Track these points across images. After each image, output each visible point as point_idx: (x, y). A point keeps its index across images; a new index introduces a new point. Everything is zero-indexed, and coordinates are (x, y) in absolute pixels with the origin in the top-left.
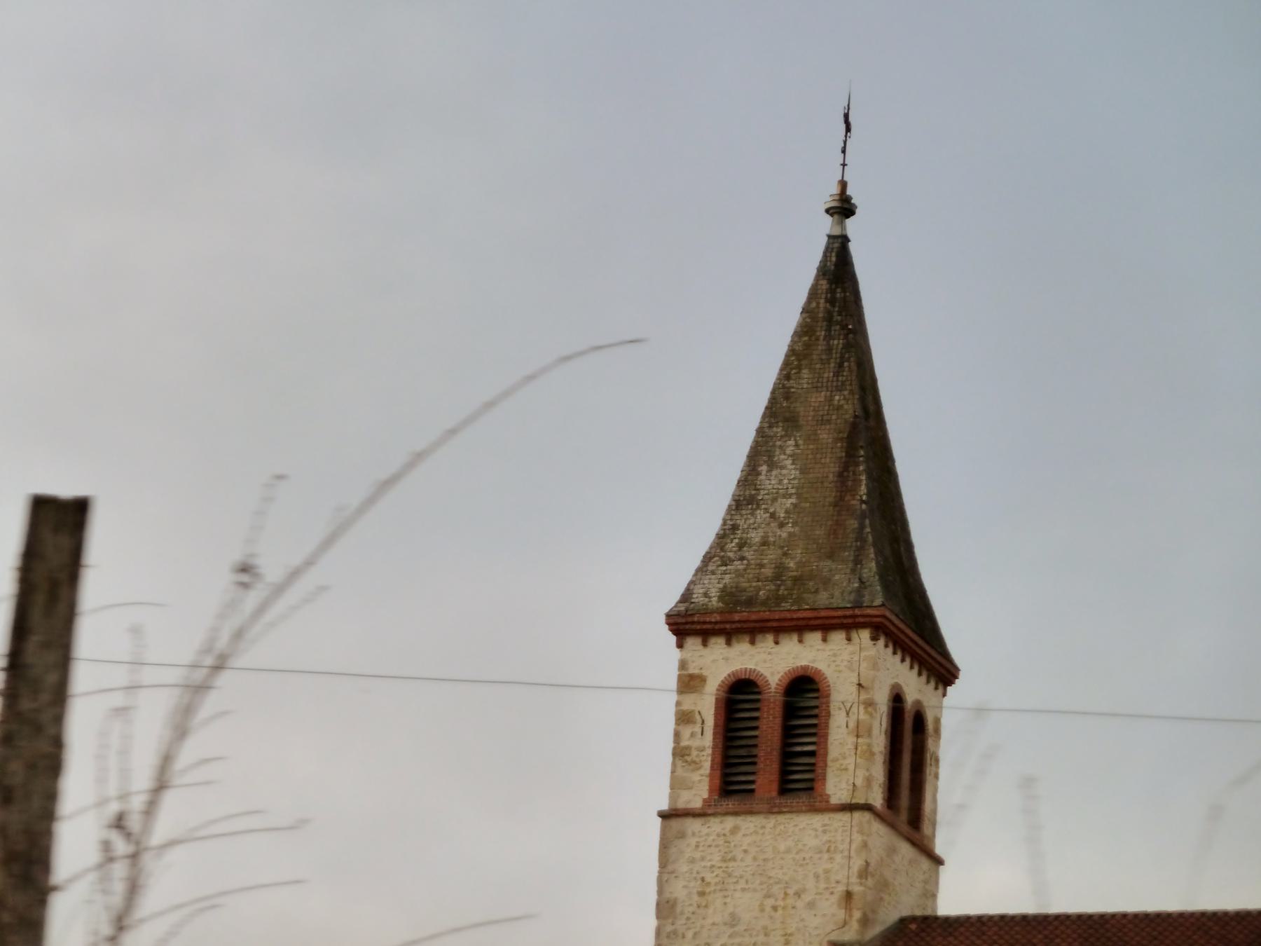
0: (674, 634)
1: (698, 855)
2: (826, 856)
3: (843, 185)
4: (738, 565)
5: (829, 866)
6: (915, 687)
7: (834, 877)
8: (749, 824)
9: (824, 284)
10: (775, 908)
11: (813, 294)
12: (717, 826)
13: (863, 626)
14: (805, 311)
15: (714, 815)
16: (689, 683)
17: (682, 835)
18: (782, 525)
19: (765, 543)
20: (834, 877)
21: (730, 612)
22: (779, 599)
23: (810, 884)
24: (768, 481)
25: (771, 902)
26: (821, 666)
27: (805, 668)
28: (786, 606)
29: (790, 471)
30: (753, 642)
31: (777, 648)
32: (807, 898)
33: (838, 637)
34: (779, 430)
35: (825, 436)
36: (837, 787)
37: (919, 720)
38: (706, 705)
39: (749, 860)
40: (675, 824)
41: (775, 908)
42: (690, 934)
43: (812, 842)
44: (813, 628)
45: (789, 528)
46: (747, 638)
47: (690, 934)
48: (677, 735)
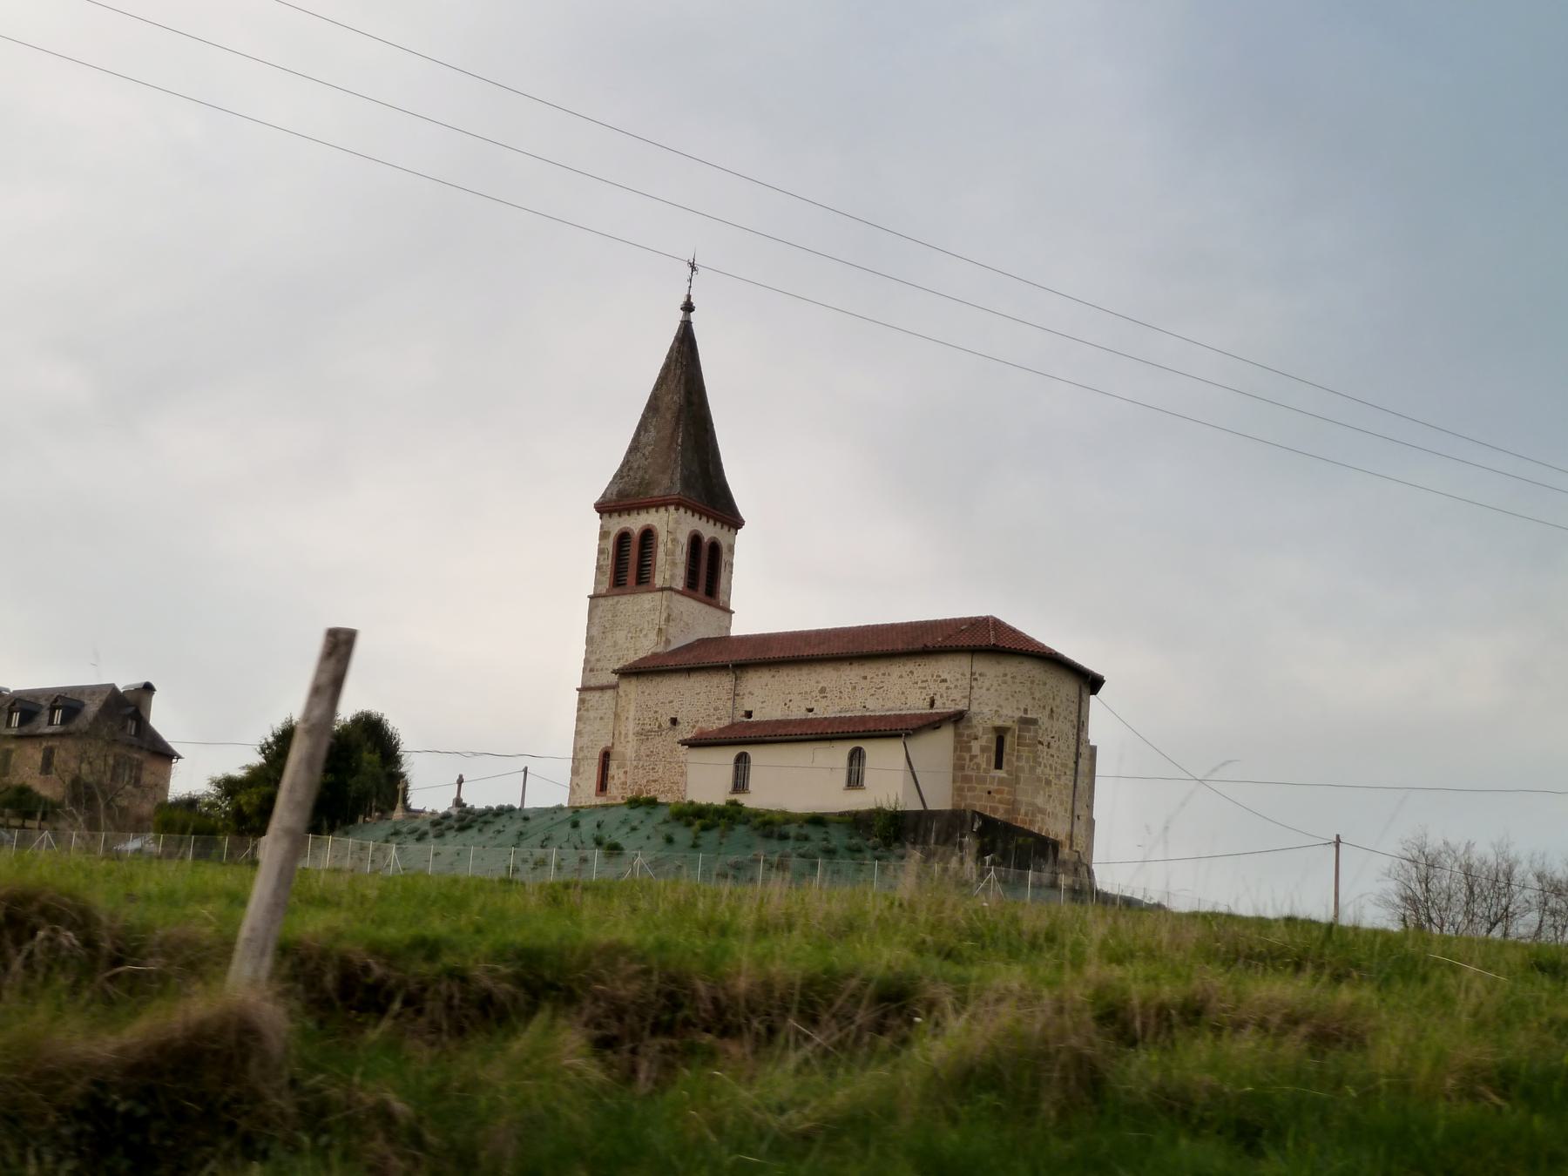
0: (598, 512)
1: (603, 615)
2: (652, 612)
3: (689, 297)
4: (626, 479)
5: (653, 617)
6: (709, 531)
7: (655, 622)
8: (624, 599)
9: (677, 344)
10: (632, 638)
11: (672, 349)
12: (611, 601)
13: (671, 504)
14: (667, 357)
15: (610, 596)
16: (604, 535)
17: (597, 606)
18: (646, 459)
19: (639, 468)
20: (655, 622)
21: (619, 501)
22: (639, 494)
23: (646, 625)
24: (643, 439)
25: (630, 635)
26: (655, 524)
27: (649, 525)
28: (641, 496)
29: (653, 433)
30: (629, 515)
31: (638, 517)
32: (644, 632)
33: (662, 510)
34: (650, 414)
35: (668, 416)
36: (658, 581)
37: (715, 548)
38: (610, 545)
39: (623, 616)
40: (595, 601)
41: (632, 638)
42: (598, 652)
43: (647, 606)
44: (653, 506)
45: (649, 460)
46: (626, 512)
47: (598, 652)
48: (598, 559)
